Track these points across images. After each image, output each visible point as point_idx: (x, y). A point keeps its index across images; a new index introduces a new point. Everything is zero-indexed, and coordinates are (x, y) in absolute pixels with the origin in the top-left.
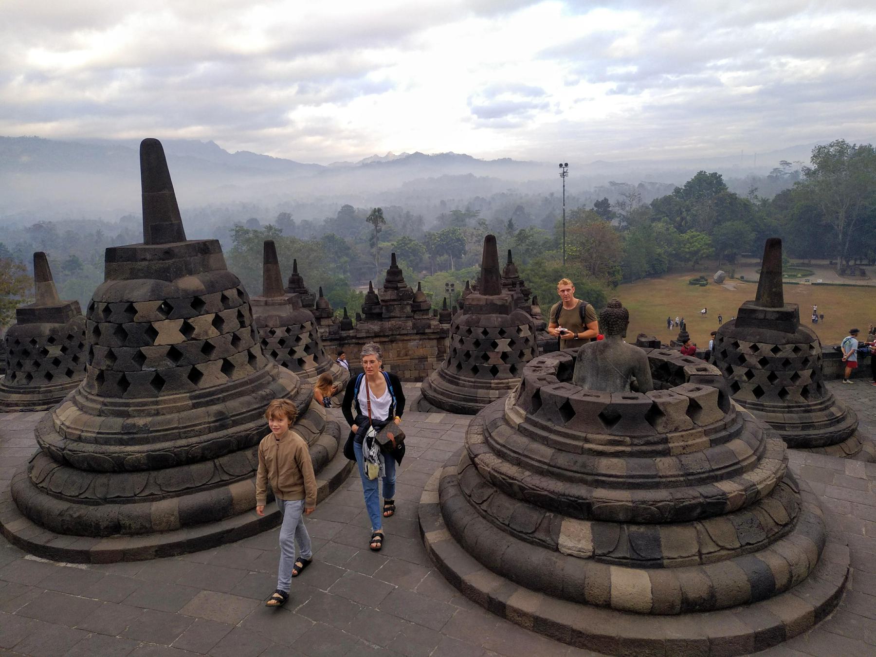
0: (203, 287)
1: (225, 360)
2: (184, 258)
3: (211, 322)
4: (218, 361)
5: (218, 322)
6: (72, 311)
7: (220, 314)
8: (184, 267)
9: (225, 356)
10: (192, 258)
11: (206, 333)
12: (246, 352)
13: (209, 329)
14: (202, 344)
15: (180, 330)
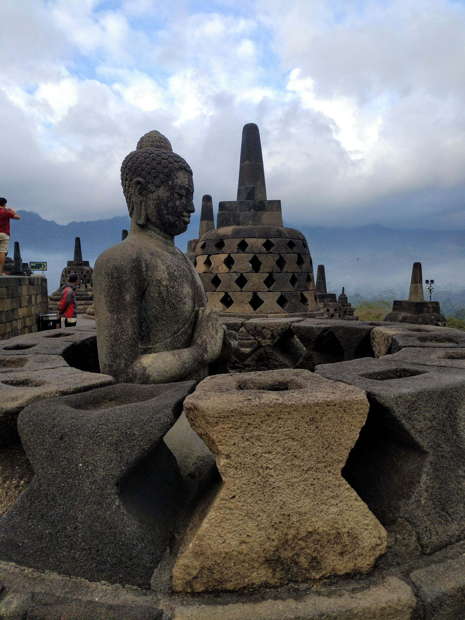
0: (230, 233)
1: (226, 294)
2: (234, 212)
3: (223, 260)
4: (221, 293)
5: (229, 262)
6: (427, 307)
7: (232, 255)
8: (232, 218)
9: (227, 290)
10: (242, 213)
11: (218, 268)
12: (251, 294)
13: (220, 266)
14: (213, 276)
15: (204, 263)
